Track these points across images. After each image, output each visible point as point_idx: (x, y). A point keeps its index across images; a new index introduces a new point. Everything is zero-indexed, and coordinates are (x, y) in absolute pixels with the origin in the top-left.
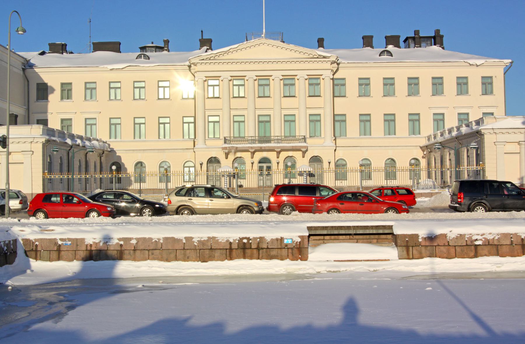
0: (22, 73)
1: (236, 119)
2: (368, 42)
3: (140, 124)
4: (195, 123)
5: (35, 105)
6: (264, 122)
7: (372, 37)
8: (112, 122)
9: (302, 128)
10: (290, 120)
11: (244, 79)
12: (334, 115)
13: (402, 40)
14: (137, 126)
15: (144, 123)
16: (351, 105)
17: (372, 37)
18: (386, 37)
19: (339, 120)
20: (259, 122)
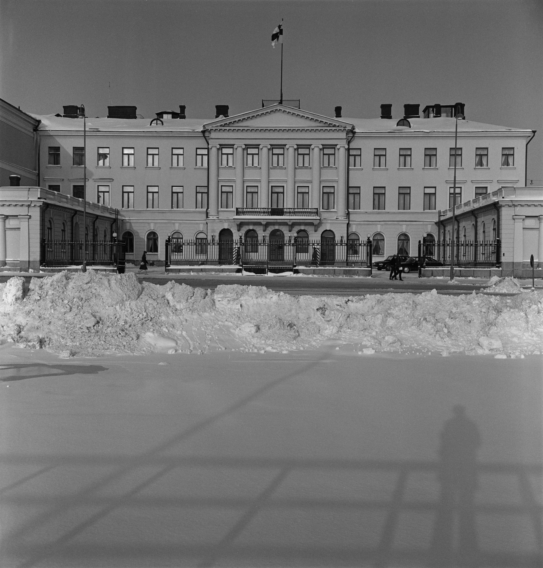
1: (224, 189)
2: (386, 112)
3: (128, 192)
4: (208, 193)
6: (276, 192)
7: (391, 105)
8: (125, 190)
9: (314, 202)
10: (302, 194)
11: (258, 148)
12: (348, 187)
13: (421, 109)
14: (126, 195)
15: (157, 192)
16: (366, 178)
17: (391, 105)
18: (406, 106)
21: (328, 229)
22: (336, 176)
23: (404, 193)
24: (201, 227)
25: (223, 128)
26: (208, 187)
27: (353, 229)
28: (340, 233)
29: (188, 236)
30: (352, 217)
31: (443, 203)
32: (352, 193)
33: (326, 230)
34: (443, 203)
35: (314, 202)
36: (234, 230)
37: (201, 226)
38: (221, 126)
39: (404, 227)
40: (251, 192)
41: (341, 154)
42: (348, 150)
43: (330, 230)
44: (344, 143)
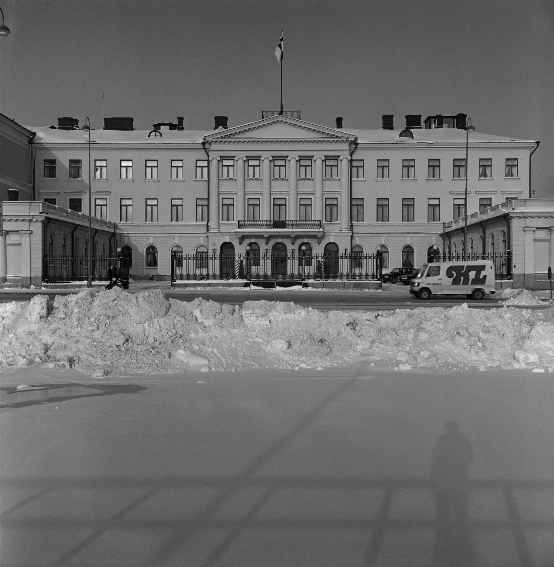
1: (225, 202)
2: (388, 123)
3: (126, 206)
4: (208, 206)
6: (278, 205)
7: (392, 116)
8: (123, 204)
9: (317, 214)
10: (305, 206)
11: (260, 160)
12: (352, 199)
13: (423, 119)
14: (124, 208)
15: (157, 205)
16: (369, 189)
17: (392, 116)
18: (407, 117)
19: (356, 205)
22: (339, 188)
23: (408, 204)
24: (202, 241)
25: (224, 140)
26: (208, 199)
27: (357, 241)
28: (344, 246)
29: (188, 250)
30: (355, 229)
31: (447, 214)
32: (356, 205)
33: (330, 243)
34: (447, 214)
35: (317, 214)
36: (236, 244)
37: (202, 239)
38: (222, 137)
39: (409, 238)
40: (253, 205)
41: (344, 165)
42: (351, 161)
43: (333, 243)
44: (347, 155)
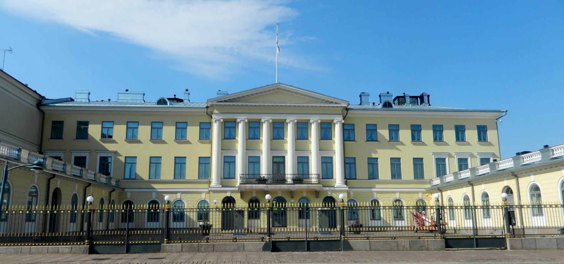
0: (36, 109)
5: (48, 143)
20: (273, 163)
21: (329, 196)
42: (343, 124)
44: (340, 118)
